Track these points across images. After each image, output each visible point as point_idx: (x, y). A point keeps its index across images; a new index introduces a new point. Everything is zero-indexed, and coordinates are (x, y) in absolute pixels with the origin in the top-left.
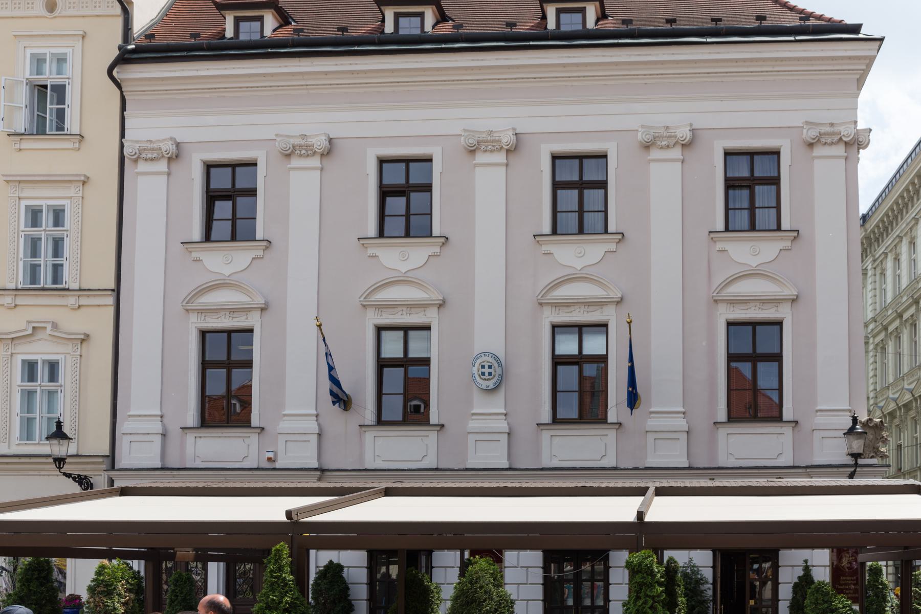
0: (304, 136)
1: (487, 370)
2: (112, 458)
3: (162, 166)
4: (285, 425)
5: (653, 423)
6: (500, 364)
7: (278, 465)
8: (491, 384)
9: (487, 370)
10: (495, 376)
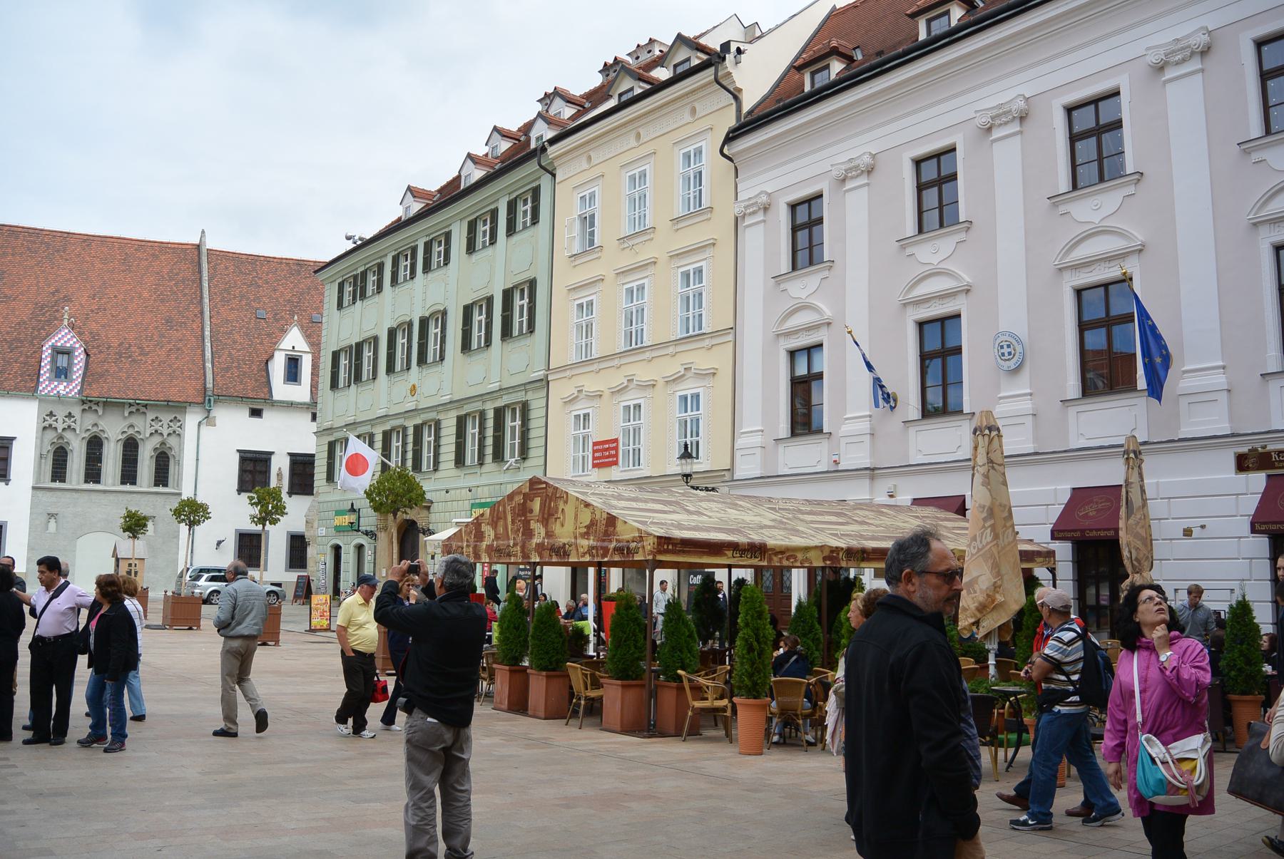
0: (850, 160)
1: (1006, 350)
2: (730, 470)
3: (760, 217)
4: (846, 428)
5: (1186, 384)
6: (1019, 341)
7: (840, 468)
8: (1012, 364)
9: (1006, 350)
10: (1013, 358)
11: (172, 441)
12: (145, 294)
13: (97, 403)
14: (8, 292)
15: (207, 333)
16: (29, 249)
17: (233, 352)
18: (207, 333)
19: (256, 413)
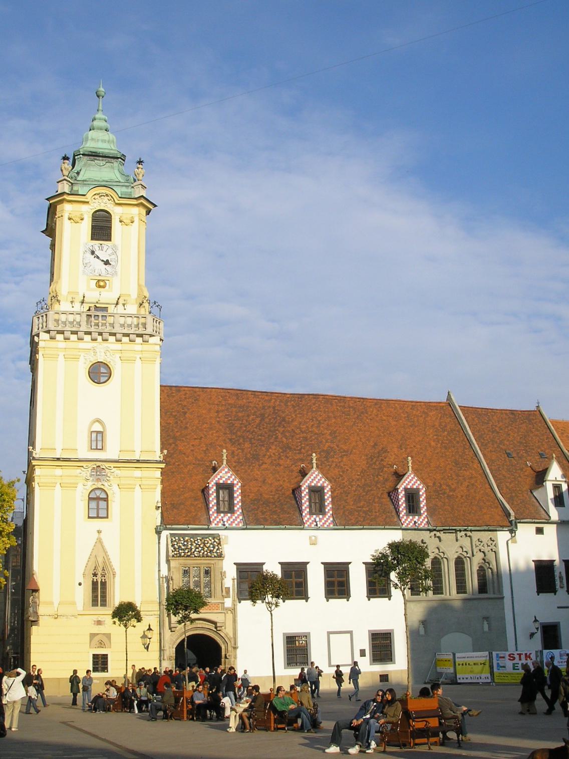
11: (491, 557)
12: (433, 444)
13: (439, 531)
14: (345, 448)
15: (488, 471)
16: (343, 413)
17: (508, 484)
18: (488, 471)
19: (540, 531)
